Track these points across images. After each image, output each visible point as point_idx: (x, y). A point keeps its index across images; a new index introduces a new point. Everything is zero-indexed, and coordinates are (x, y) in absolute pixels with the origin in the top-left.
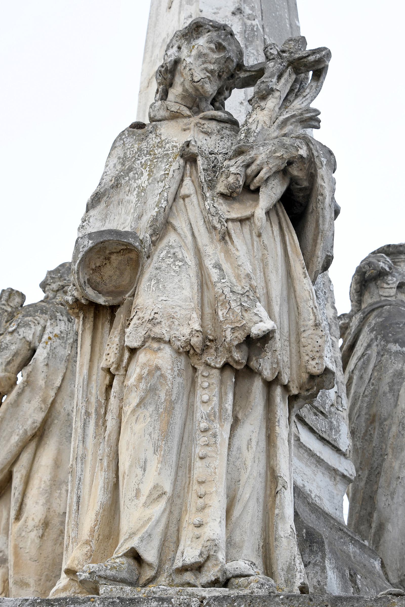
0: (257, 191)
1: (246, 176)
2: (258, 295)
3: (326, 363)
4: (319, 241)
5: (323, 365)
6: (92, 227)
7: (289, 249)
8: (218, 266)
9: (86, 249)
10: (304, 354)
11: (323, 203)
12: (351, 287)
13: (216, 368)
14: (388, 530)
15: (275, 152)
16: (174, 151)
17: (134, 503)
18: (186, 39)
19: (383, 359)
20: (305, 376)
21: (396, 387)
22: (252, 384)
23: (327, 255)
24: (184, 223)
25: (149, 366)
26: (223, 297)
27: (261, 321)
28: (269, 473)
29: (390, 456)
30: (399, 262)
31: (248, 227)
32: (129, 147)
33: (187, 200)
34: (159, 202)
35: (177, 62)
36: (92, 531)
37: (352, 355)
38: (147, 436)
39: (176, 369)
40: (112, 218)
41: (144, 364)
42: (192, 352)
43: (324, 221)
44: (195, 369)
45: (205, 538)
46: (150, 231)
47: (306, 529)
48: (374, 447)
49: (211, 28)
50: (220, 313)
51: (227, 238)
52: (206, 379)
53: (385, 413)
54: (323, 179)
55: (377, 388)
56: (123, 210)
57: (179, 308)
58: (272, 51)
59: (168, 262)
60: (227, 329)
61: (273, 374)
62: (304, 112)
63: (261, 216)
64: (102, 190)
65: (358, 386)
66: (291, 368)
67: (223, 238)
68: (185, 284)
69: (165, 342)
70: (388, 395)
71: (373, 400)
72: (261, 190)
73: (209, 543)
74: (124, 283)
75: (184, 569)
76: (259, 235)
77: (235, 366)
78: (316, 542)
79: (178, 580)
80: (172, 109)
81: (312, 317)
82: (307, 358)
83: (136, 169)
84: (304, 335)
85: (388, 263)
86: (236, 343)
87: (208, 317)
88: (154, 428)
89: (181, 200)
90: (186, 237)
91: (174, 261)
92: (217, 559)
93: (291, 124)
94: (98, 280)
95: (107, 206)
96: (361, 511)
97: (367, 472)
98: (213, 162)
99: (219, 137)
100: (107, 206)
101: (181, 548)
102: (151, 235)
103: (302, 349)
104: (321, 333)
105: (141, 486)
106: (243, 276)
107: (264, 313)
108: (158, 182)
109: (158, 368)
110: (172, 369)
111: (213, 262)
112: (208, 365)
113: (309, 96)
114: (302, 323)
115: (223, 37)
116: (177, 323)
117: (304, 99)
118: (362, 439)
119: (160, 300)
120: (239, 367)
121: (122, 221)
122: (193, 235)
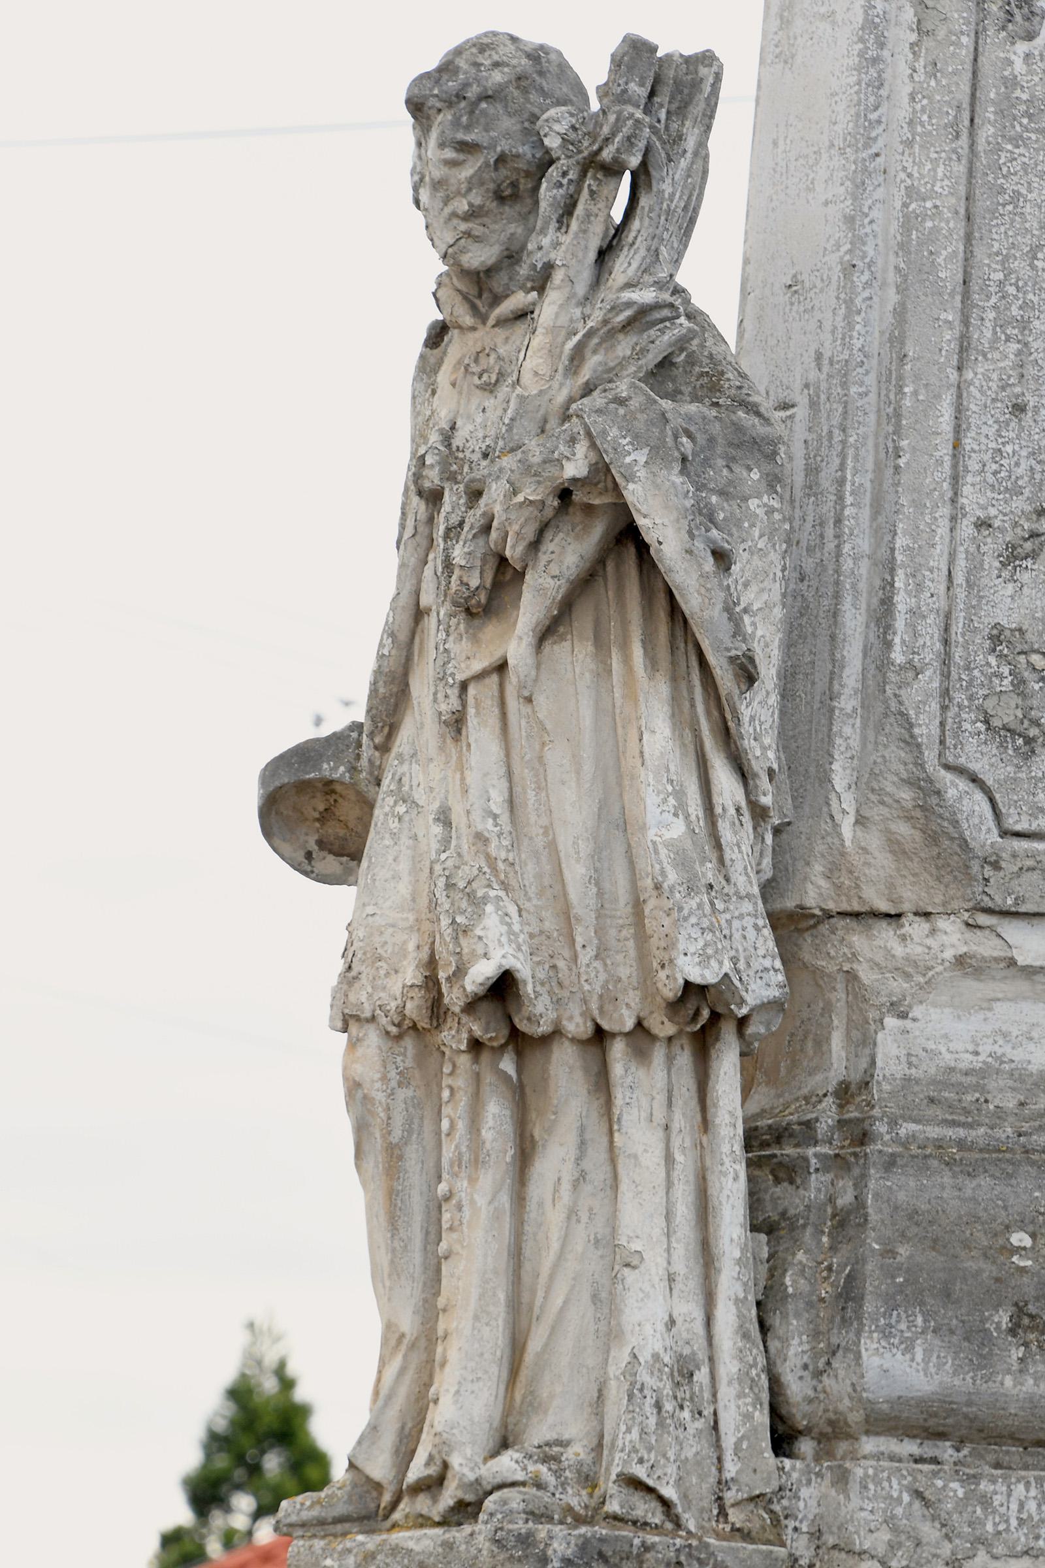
3: (681, 971)
5: (675, 979)
22: (548, 1061)
23: (731, 657)
39: (393, 1074)
57: (390, 930)
62: (610, 316)
93: (595, 352)
94: (342, 832)
110: (384, 1079)
113: (639, 239)
117: (632, 251)
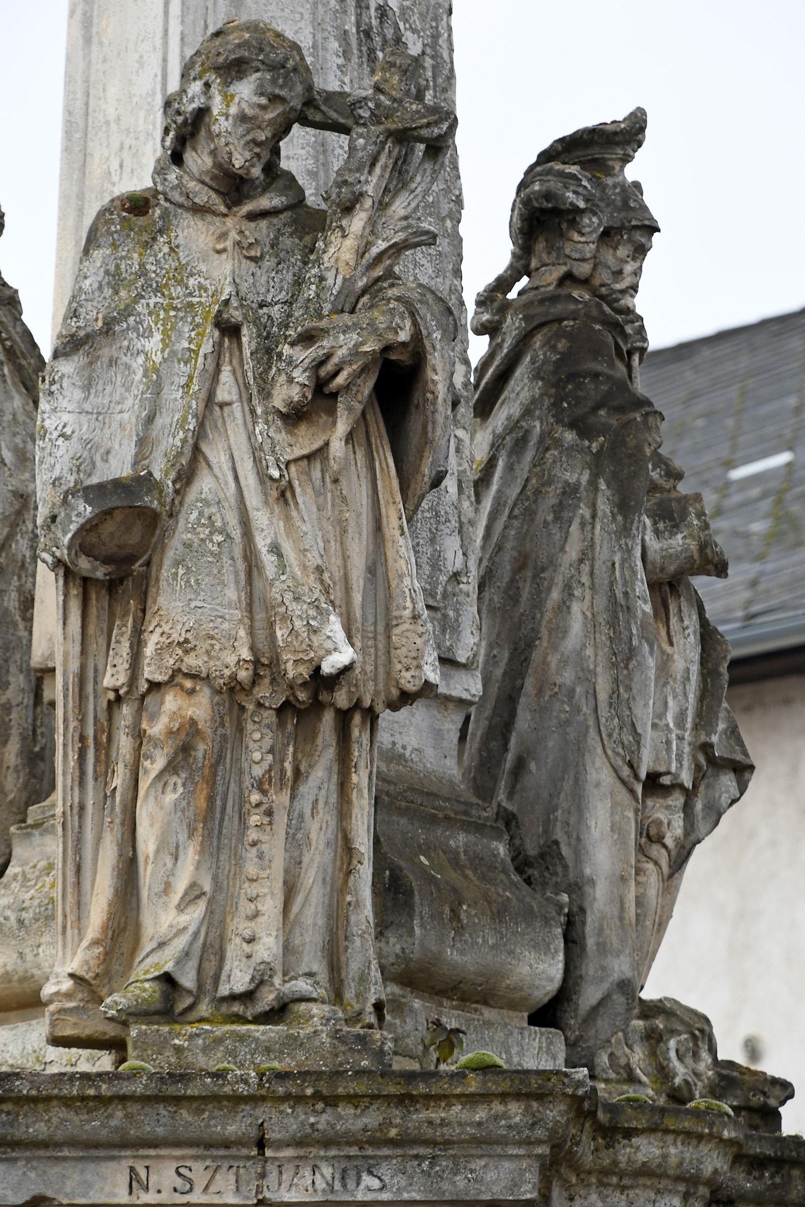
0: (334, 396)
1: (318, 377)
2: (332, 597)
4: (426, 454)
6: (67, 399)
7: (379, 483)
8: (275, 549)
9: (81, 520)
10: (395, 661)
11: (434, 403)
12: (513, 210)
13: (271, 708)
14: (531, 772)
15: (362, 344)
16: (203, 300)
17: (162, 900)
18: (220, 76)
19: (547, 455)
20: (395, 692)
21: (566, 514)
22: (320, 720)
24: (222, 453)
25: (181, 717)
26: (283, 609)
27: (335, 649)
28: (340, 836)
29: (545, 644)
30: (611, 159)
31: (318, 465)
32: (124, 253)
33: (226, 410)
34: (184, 420)
35: (202, 113)
36: (105, 928)
37: (500, 401)
38: (179, 814)
40: (100, 387)
41: (174, 713)
42: (238, 688)
43: (434, 428)
44: (242, 709)
45: (257, 959)
46: (173, 475)
47: (392, 871)
48: (522, 615)
49: (261, 67)
50: (279, 633)
51: (288, 495)
52: (257, 726)
53: (544, 559)
54: (435, 370)
55: (534, 507)
56: (119, 379)
57: (220, 620)
58: (361, 112)
59: (202, 536)
60: (288, 660)
61: (350, 700)
63: (338, 454)
64: (82, 333)
65: (506, 482)
66: (375, 679)
67: (283, 494)
68: (229, 578)
69: (202, 679)
70: (551, 527)
71: (526, 527)
72: (339, 399)
73: (262, 967)
74: (131, 542)
75: (233, 998)
76: (336, 481)
77: (298, 705)
78: (402, 893)
79: (224, 1009)
80: (197, 200)
81: (409, 604)
82: (399, 667)
83: (139, 314)
84: (396, 631)
85: (585, 192)
86: (300, 681)
87: (261, 635)
88: (188, 803)
89: (217, 409)
90: (226, 483)
91: (211, 533)
92: (272, 985)
93: (389, 258)
94: (94, 540)
95: (91, 363)
96: (492, 718)
97: (506, 654)
98: (265, 327)
99: (274, 261)
100: (91, 363)
101: (227, 968)
102: (174, 482)
103: (393, 651)
104: (421, 630)
105: (171, 879)
106: (311, 570)
107: (340, 635)
108: (179, 362)
109: (193, 722)
111: (269, 541)
112: (260, 705)
113: (419, 189)
114: (394, 614)
115: (281, 81)
116: (217, 647)
117: (412, 196)
118: (504, 592)
119: (192, 606)
120: (302, 707)
121: (117, 397)
122: (236, 478)
